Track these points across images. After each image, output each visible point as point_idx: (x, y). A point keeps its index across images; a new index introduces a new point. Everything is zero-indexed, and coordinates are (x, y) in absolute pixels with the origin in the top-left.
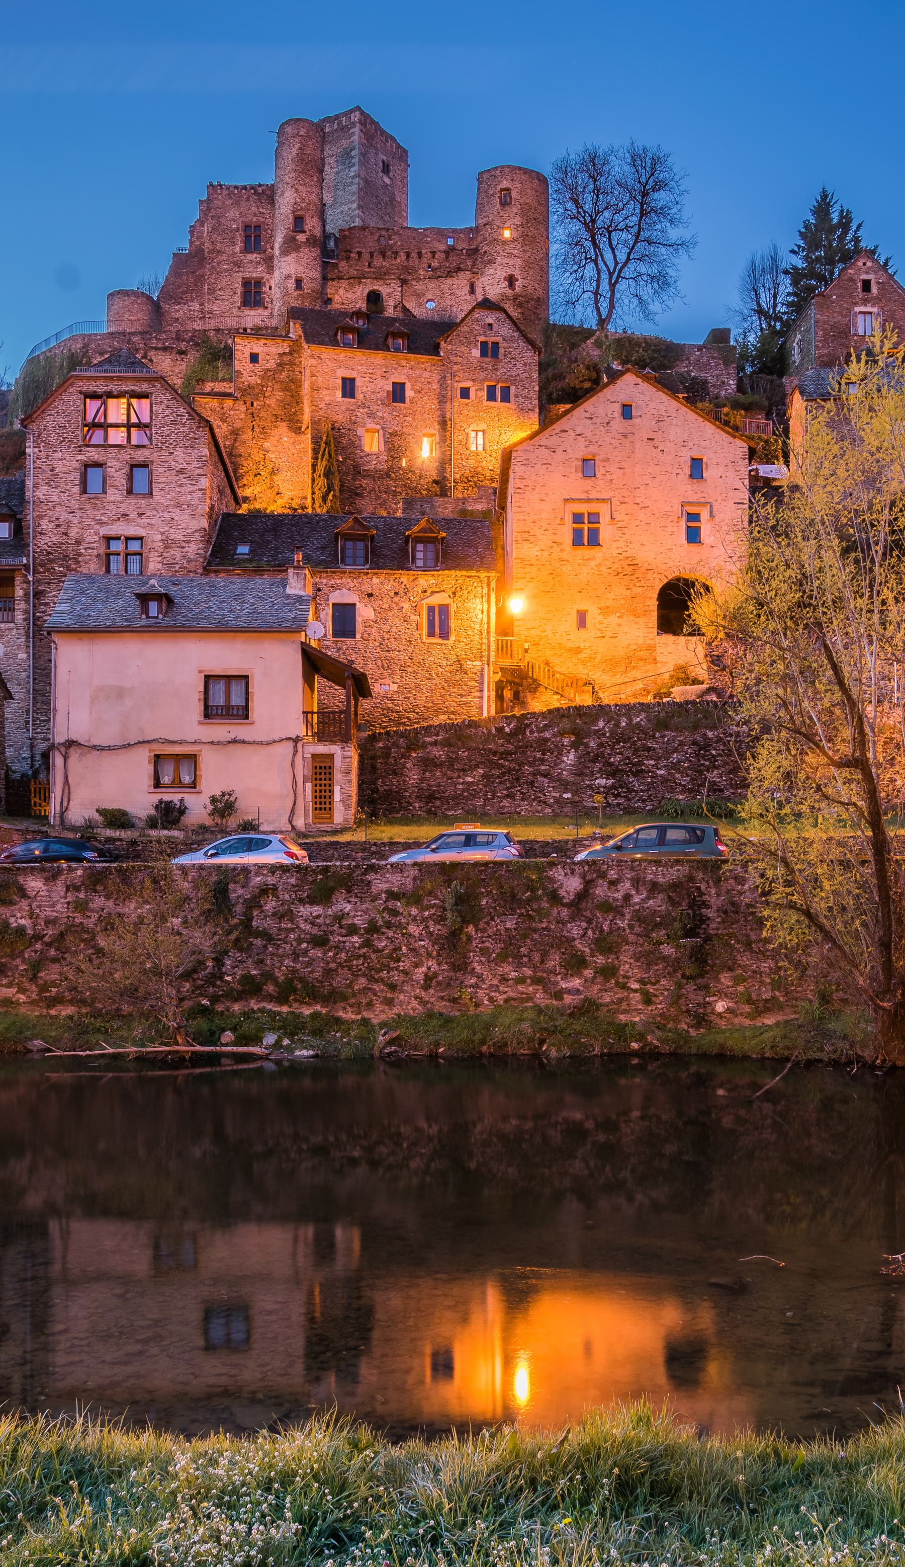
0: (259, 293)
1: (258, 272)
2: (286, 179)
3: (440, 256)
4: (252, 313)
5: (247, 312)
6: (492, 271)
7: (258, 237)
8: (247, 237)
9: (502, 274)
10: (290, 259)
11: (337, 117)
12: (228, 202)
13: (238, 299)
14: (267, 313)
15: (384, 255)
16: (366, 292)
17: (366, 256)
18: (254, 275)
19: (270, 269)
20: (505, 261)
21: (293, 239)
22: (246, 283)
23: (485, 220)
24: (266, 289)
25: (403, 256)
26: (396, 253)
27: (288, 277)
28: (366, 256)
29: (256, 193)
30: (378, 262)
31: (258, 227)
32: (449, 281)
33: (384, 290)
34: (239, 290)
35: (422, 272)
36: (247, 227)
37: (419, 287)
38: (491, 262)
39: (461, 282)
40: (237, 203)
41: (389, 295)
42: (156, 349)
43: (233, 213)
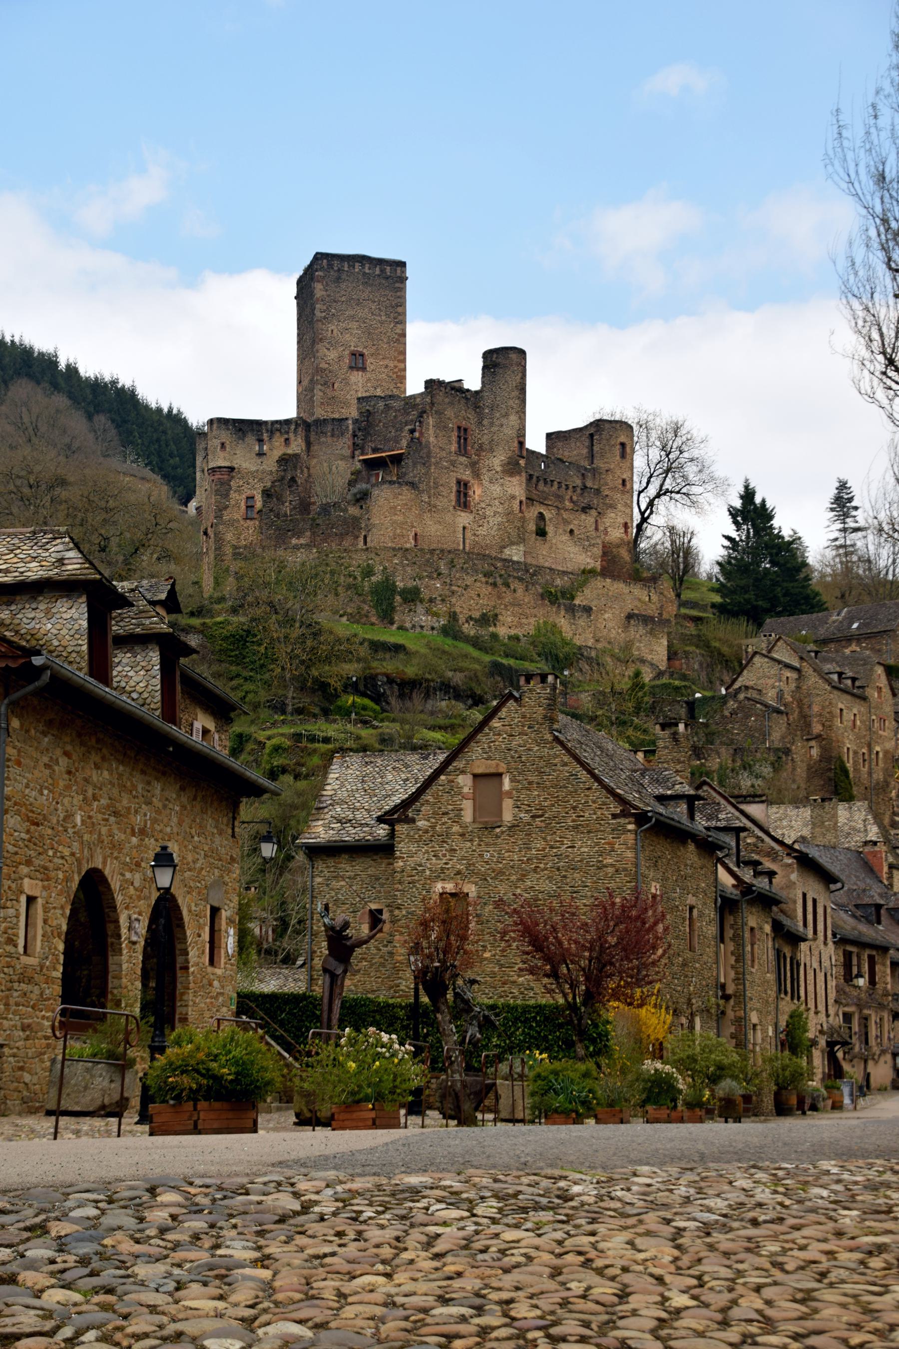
0: (466, 495)
1: (466, 475)
2: (511, 403)
3: (579, 491)
4: (463, 514)
5: (459, 513)
6: (613, 515)
7: (465, 439)
8: (459, 437)
9: (621, 520)
10: (515, 480)
11: (381, 262)
12: (447, 400)
13: (453, 497)
14: (471, 517)
15: (545, 482)
16: (536, 513)
17: (535, 479)
18: (464, 477)
19: (477, 475)
20: (623, 509)
21: (518, 464)
22: (459, 482)
23: (606, 466)
24: (471, 493)
25: (556, 484)
26: (552, 481)
27: (513, 497)
28: (535, 479)
29: (467, 399)
30: (541, 486)
31: (465, 430)
32: (583, 516)
33: (547, 515)
34: (454, 489)
35: (568, 504)
36: (459, 428)
37: (565, 515)
38: (613, 507)
39: (589, 520)
40: (451, 403)
41: (550, 519)
42: (515, 577)
43: (449, 413)
